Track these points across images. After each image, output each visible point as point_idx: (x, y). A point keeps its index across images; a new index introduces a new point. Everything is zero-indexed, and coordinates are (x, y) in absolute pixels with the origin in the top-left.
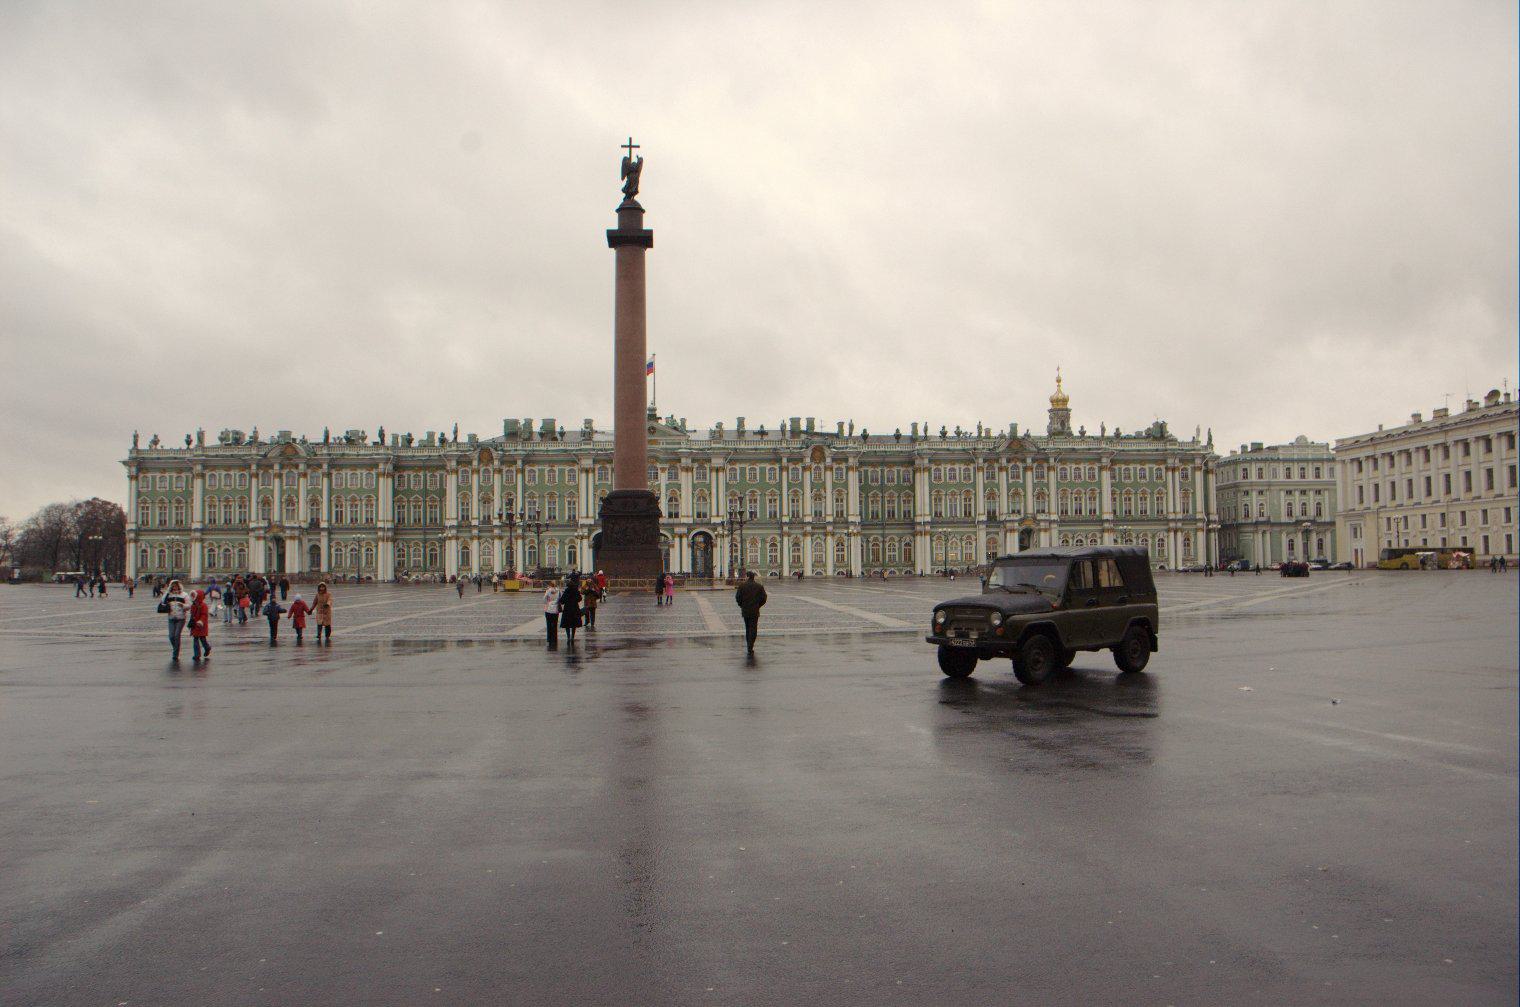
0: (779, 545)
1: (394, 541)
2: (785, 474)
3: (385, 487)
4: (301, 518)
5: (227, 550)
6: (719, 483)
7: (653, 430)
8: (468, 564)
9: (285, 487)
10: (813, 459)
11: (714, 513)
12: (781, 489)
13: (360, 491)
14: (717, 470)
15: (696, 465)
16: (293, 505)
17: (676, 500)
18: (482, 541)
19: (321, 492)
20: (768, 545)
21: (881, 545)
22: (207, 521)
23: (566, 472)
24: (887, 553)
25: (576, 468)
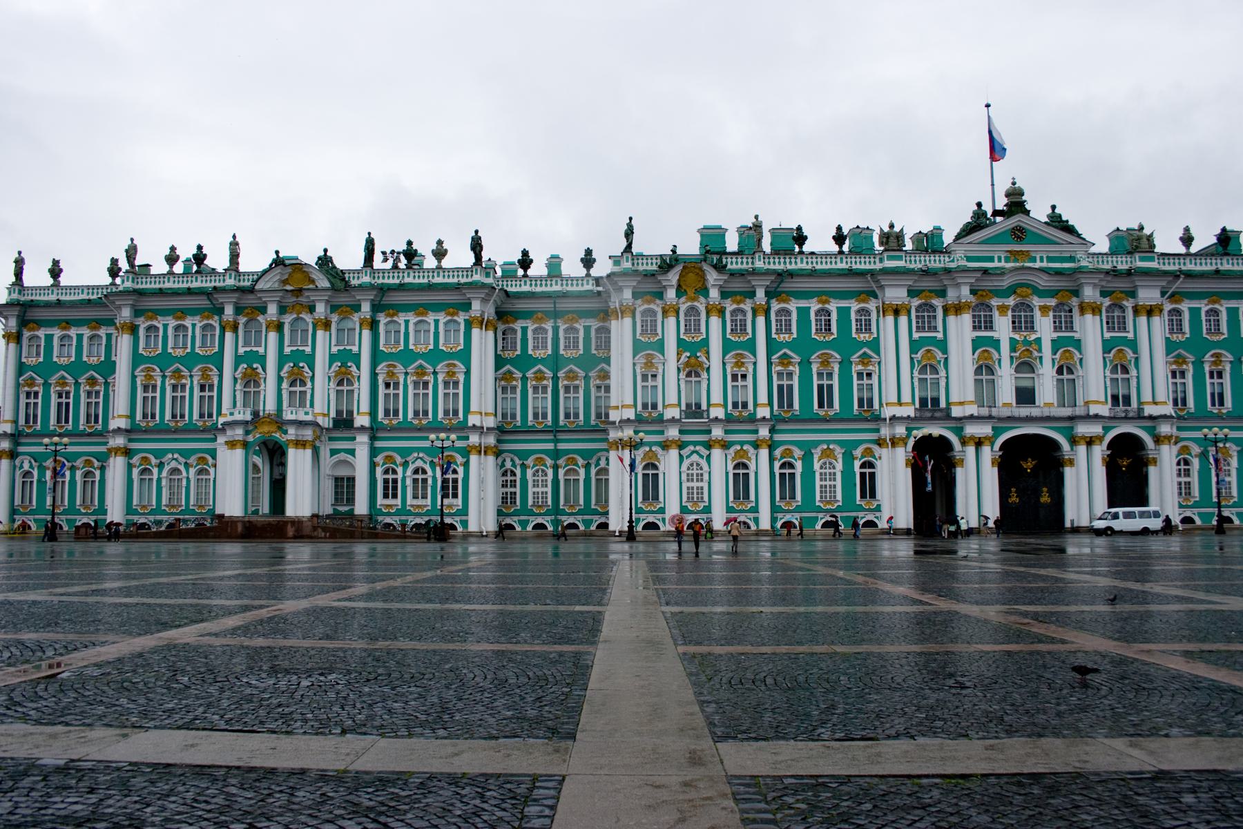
1: (498, 454)
3: (483, 344)
4: (318, 408)
5: (175, 471)
7: (1019, 234)
8: (656, 498)
9: (287, 350)
11: (1147, 396)
13: (436, 355)
15: (1107, 302)
16: (303, 383)
17: (1070, 371)
18: (685, 452)
19: (357, 358)
22: (139, 416)
25: (872, 305)
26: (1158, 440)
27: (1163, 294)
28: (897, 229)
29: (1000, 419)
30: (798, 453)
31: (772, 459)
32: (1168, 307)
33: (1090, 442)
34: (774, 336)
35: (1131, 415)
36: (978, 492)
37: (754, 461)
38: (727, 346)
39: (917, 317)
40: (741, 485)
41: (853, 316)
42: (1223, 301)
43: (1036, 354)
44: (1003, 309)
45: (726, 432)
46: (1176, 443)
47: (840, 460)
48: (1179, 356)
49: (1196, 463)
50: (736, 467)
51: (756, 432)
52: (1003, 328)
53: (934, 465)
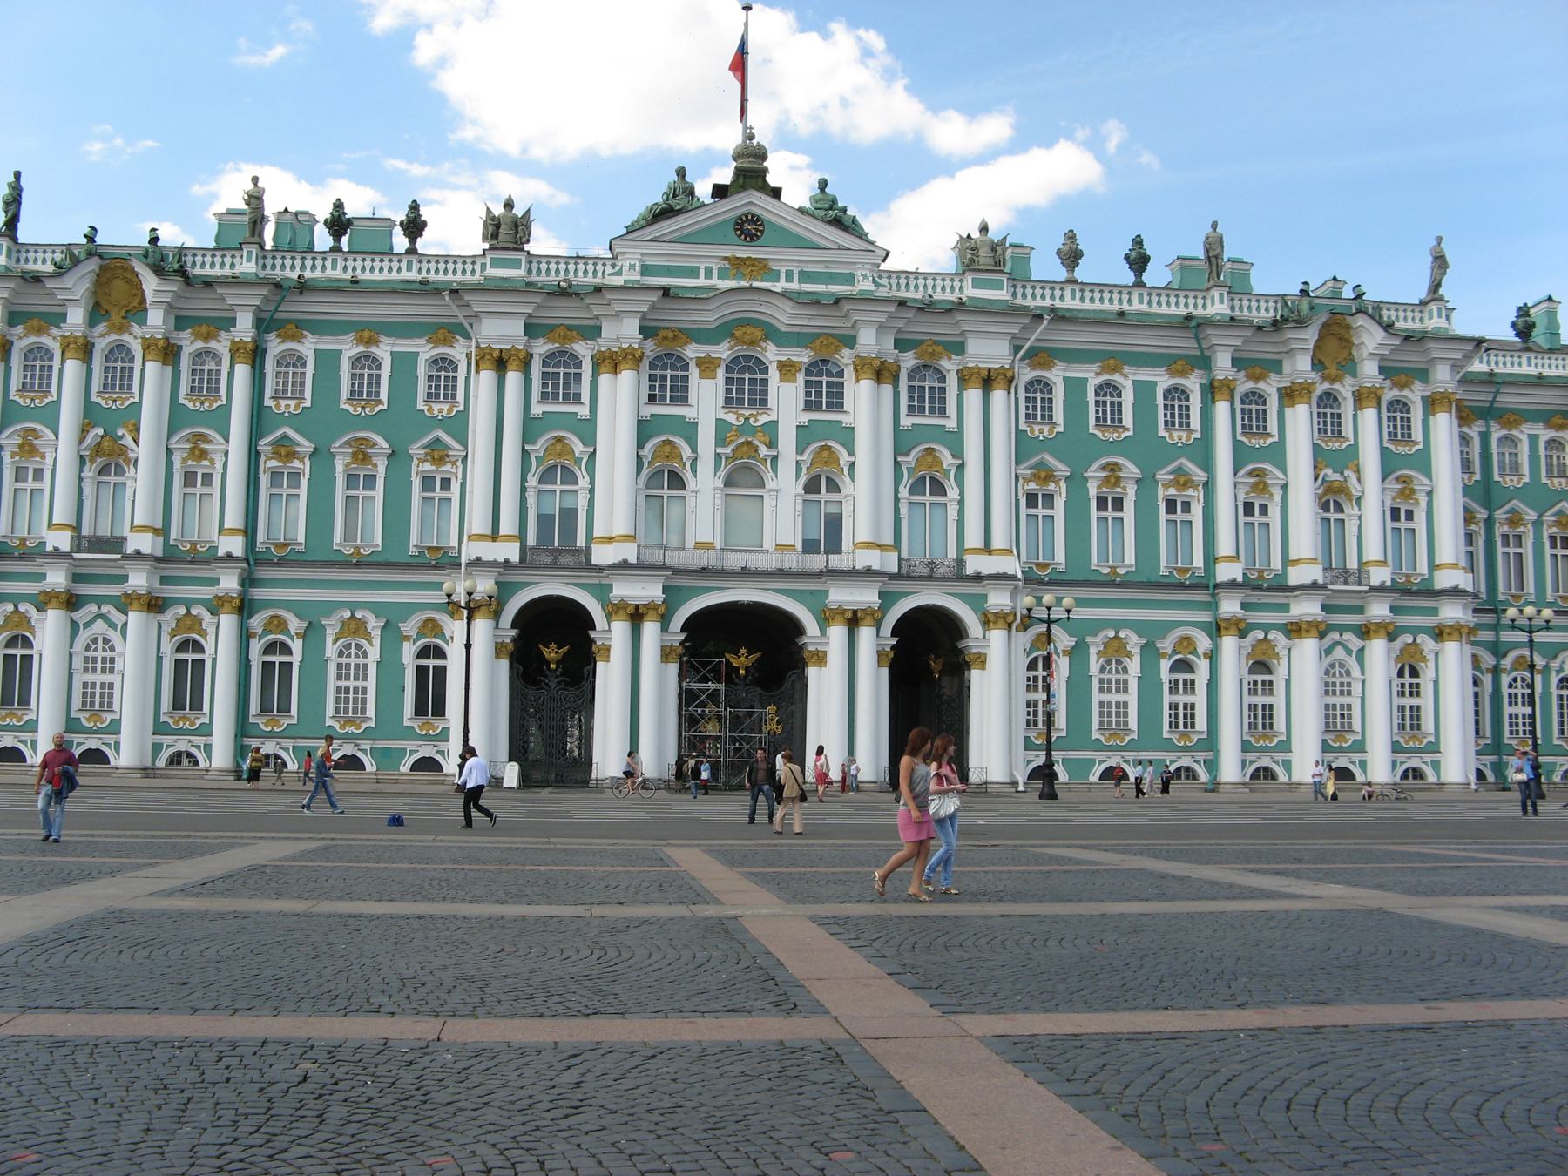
0: (1203, 667)
2: (1222, 408)
6: (986, 427)
7: (749, 228)
10: (1317, 364)
11: (974, 538)
12: (1207, 464)
14: (988, 382)
15: (909, 360)
17: (833, 487)
18: (81, 615)
20: (1165, 665)
21: (1487, 680)
23: (422, 371)
24: (1507, 710)
25: (459, 351)
26: (987, 621)
27: (1017, 349)
28: (518, 211)
29: (677, 571)
30: (295, 625)
31: (245, 636)
32: (1026, 374)
33: (853, 621)
34: (268, 402)
35: (941, 571)
36: (633, 709)
37: (211, 638)
38: (177, 418)
39: (545, 375)
40: (188, 685)
41: (422, 371)
42: (1127, 369)
43: (763, 451)
44: (707, 366)
45: (165, 580)
46: (1025, 627)
47: (377, 641)
48: (1041, 466)
49: (1062, 666)
50: (182, 647)
51: (216, 581)
52: (706, 399)
53: (551, 654)
